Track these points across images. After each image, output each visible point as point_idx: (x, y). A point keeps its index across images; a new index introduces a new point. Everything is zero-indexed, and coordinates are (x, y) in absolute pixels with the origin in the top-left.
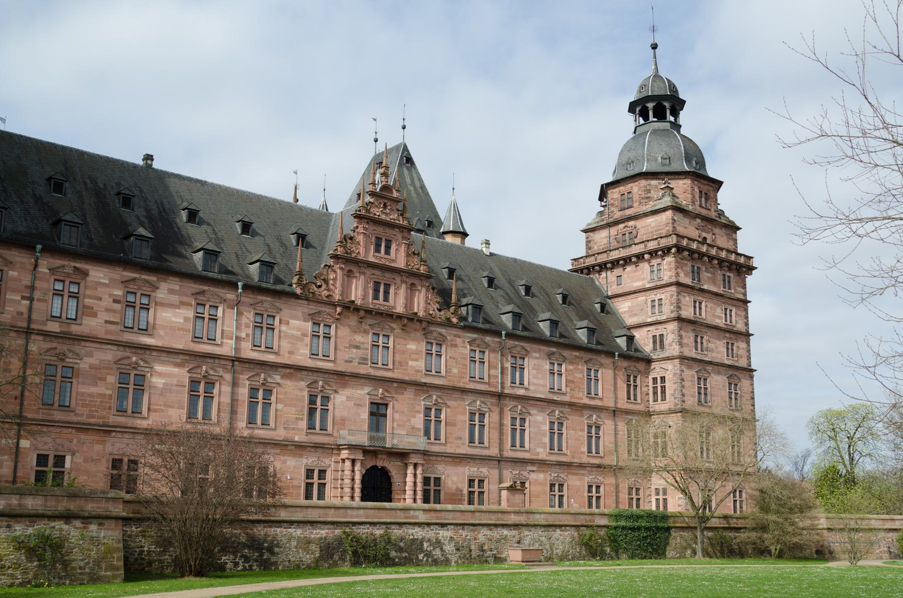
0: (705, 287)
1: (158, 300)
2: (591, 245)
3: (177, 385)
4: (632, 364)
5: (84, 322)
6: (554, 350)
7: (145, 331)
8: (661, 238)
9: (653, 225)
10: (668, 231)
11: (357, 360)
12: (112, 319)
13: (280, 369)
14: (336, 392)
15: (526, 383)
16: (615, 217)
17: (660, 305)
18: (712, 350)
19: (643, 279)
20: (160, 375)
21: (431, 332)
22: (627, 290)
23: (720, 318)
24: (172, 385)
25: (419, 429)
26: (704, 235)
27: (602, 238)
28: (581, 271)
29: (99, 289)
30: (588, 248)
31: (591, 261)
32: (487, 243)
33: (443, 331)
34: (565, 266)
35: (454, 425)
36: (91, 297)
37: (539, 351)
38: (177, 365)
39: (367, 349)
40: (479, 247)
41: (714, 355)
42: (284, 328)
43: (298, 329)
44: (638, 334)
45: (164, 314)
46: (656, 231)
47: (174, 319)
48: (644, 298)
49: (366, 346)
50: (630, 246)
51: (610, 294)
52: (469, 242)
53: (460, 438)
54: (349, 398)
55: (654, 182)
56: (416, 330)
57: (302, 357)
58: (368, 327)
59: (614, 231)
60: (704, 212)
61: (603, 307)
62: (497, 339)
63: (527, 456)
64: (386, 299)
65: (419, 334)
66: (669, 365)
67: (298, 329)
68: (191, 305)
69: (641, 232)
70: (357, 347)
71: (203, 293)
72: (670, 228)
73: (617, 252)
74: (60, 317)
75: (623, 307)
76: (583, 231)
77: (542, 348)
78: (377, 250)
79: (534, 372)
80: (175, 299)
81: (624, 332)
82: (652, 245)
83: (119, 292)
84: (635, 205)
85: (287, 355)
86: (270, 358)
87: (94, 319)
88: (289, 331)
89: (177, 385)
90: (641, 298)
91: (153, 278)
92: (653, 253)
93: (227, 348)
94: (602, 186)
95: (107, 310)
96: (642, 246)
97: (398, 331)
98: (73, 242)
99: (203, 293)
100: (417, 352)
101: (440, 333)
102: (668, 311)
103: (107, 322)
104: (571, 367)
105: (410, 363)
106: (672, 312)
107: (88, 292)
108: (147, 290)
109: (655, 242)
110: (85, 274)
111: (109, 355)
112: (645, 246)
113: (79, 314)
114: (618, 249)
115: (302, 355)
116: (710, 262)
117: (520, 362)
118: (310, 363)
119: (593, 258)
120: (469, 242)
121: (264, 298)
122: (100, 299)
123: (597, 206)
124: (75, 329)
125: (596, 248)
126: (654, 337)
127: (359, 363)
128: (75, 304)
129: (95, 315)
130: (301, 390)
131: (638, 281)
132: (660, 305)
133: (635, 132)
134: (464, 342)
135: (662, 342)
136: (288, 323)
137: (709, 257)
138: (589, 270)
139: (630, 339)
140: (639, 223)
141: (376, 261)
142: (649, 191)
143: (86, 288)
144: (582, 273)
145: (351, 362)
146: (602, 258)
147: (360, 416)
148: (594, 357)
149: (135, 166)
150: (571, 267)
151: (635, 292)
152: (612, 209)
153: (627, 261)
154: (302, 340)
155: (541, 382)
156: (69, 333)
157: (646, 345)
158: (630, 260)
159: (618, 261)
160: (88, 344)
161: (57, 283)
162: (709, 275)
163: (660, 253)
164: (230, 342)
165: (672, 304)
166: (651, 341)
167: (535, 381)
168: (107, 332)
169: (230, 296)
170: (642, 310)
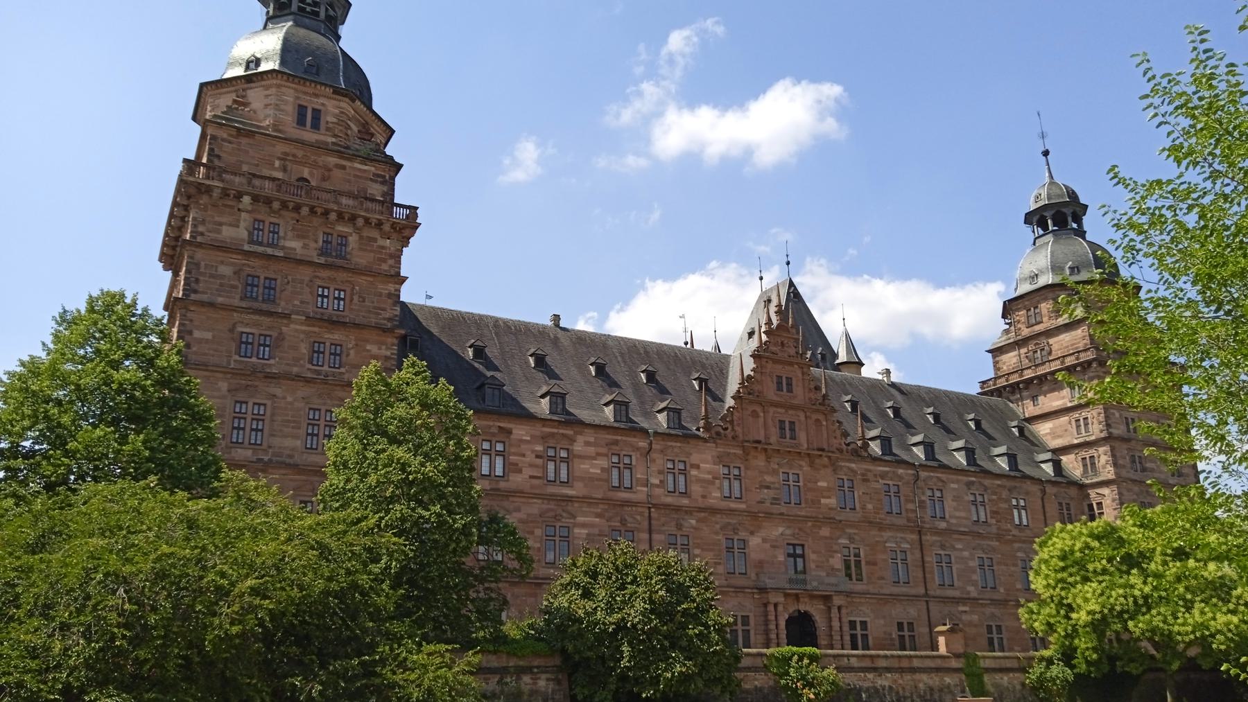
1: (575, 453)
2: (1000, 365)
3: (599, 535)
4: (1063, 490)
5: (511, 478)
6: (973, 479)
7: (566, 484)
8: (1078, 352)
9: (1067, 339)
10: (1086, 344)
11: (769, 501)
12: (535, 474)
13: (695, 514)
14: (752, 533)
15: (947, 516)
16: (1023, 334)
17: (1086, 425)
19: (1063, 398)
20: (583, 525)
21: (841, 467)
22: (1047, 411)
24: (594, 535)
25: (838, 570)
27: (1010, 360)
28: (991, 393)
29: (523, 446)
30: (997, 369)
31: (1002, 382)
32: (888, 372)
33: (853, 465)
34: (974, 389)
35: (875, 564)
36: (515, 454)
37: (957, 482)
38: (598, 515)
39: (777, 489)
40: (880, 377)
42: (694, 472)
43: (709, 473)
44: (1065, 459)
45: (582, 466)
46: (1072, 345)
47: (591, 470)
48: (1067, 418)
49: (777, 485)
50: (1043, 363)
51: (1027, 416)
52: (866, 372)
53: (882, 578)
54: (764, 540)
57: (715, 498)
58: (776, 467)
59: (1023, 351)
61: (1021, 430)
63: (957, 594)
64: (793, 438)
65: (829, 471)
66: (1105, 491)
67: (709, 473)
68: (606, 455)
69: (1055, 347)
70: (768, 487)
71: (616, 443)
72: (1087, 341)
73: (1029, 371)
74: (490, 475)
75: (1043, 429)
76: (989, 351)
78: (780, 388)
79: (955, 504)
80: (591, 450)
81: (1048, 456)
82: (1070, 361)
83: (539, 448)
84: (1045, 319)
85: (700, 499)
86: (685, 501)
87: (520, 475)
88: (702, 476)
89: (599, 535)
90: (1064, 419)
91: (570, 432)
92: (1070, 370)
93: (641, 493)
94: (1005, 302)
95: (531, 465)
96: (1058, 362)
97: (806, 468)
98: (497, 403)
99: (616, 443)
100: (828, 489)
101: (849, 468)
102: (1096, 430)
103: (531, 477)
104: (994, 497)
105: (823, 501)
106: (1101, 431)
107: (513, 450)
108: (565, 444)
109: (1073, 358)
110: (509, 432)
111: (535, 507)
112: (1063, 363)
113: (506, 471)
114: (1030, 368)
115: (716, 498)
117: (938, 494)
118: (724, 504)
119: (1003, 379)
120: (866, 372)
121: (674, 444)
122: (524, 455)
123: (1002, 325)
124: (502, 485)
125: (1005, 368)
126: (1084, 459)
127: (772, 504)
128: (502, 462)
129: (520, 471)
130: (717, 533)
131: (1058, 400)
132: (1086, 425)
133: (1034, 244)
134: (875, 476)
135: (1093, 464)
136: (698, 467)
138: (998, 392)
139: (1057, 465)
140: (1051, 341)
141: (778, 399)
143: (511, 445)
144: (992, 396)
145: (763, 503)
146: (1015, 379)
147: (776, 557)
148: (1018, 485)
149: (544, 327)
150: (980, 391)
152: (1019, 326)
153: (1042, 379)
154: (713, 483)
155: (963, 514)
156: (498, 490)
157: (1074, 468)
158: (1046, 378)
159: (1031, 379)
160: (515, 499)
161: (484, 443)
163: (1078, 369)
164: (645, 489)
165: (1100, 423)
166: (1081, 464)
168: (532, 487)
169: (643, 444)
170: (1066, 430)
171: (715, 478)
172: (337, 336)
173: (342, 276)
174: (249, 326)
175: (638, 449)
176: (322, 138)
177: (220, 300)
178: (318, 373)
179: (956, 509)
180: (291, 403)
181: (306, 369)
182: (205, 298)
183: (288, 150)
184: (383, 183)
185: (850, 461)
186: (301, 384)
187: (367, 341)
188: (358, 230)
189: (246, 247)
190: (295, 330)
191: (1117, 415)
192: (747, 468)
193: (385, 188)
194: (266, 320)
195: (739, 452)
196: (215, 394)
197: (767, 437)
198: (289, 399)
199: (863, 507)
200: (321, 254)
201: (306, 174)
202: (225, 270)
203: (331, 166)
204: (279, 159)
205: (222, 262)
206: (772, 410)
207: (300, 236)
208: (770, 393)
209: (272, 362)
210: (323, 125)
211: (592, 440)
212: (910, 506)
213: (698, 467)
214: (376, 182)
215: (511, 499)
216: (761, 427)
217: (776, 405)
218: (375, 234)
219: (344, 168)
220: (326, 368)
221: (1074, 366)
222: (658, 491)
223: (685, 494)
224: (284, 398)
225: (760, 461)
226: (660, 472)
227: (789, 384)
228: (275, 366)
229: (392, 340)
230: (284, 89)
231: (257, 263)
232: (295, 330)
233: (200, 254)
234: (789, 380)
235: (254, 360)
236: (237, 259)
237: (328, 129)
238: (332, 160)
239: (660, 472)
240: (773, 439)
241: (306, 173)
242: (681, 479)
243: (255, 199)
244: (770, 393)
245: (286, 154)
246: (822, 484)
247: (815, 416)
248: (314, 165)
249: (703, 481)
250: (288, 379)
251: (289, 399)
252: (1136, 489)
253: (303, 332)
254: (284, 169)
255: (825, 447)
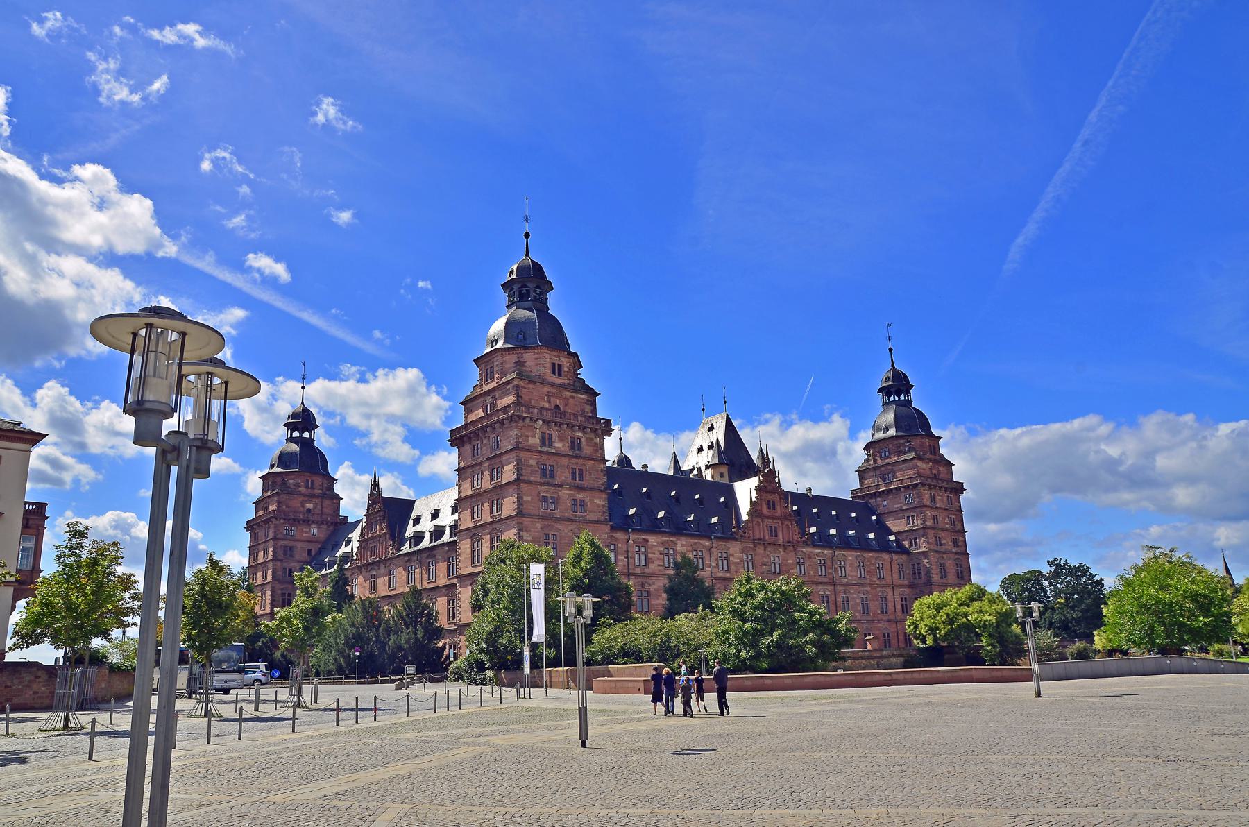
0: (938, 506)
6: (859, 554)
18: (945, 545)
19: (901, 503)
23: (947, 523)
26: (934, 472)
41: (947, 547)
55: (902, 441)
56: (791, 551)
60: (933, 457)
62: (830, 552)
64: (776, 536)
70: (765, 565)
77: (853, 553)
91: (674, 539)
100: (793, 564)
103: (659, 565)
104: (869, 563)
116: (940, 490)
122: (654, 554)
124: (646, 570)
129: (653, 562)
131: (898, 504)
134: (814, 555)
136: (732, 555)
137: (939, 487)
142: (899, 447)
151: (895, 511)
160: (652, 578)
162: (940, 497)
167: (852, 574)
168: (660, 571)
171: (741, 561)
172: (581, 496)
173: (581, 461)
174: (547, 492)
175: (704, 547)
176: (563, 381)
177: (532, 479)
178: (575, 516)
179: (851, 571)
180: (567, 534)
181: (569, 514)
182: (526, 478)
183: (549, 390)
184: (591, 405)
185: (803, 547)
186: (570, 523)
187: (594, 497)
188: (585, 433)
189: (540, 449)
190: (564, 493)
191: (929, 514)
192: (755, 555)
193: (592, 408)
194: (552, 489)
195: (752, 546)
196: (536, 530)
197: (764, 537)
198: (566, 531)
199: (809, 573)
200: (572, 447)
201: (558, 404)
202: (533, 462)
203: (568, 397)
204: (546, 395)
205: (531, 458)
206: (766, 520)
207: (562, 439)
208: (765, 510)
209: (556, 511)
210: (563, 375)
211: (684, 543)
212: (830, 571)
213: (732, 555)
214: (588, 404)
215: (650, 578)
216: (761, 532)
217: (768, 517)
218: (592, 436)
219: (573, 397)
220: (578, 513)
221: (908, 486)
222: (715, 570)
223: (728, 571)
224: (564, 531)
225: (760, 550)
226: (716, 559)
227: (774, 505)
228: (558, 513)
229: (604, 496)
230: (545, 354)
231: (545, 457)
232: (564, 493)
233: (522, 454)
234: (773, 502)
235: (549, 510)
236: (536, 455)
237: (566, 376)
238: (569, 394)
239: (716, 559)
240: (767, 538)
241: (558, 402)
242: (725, 562)
243: (544, 421)
244: (765, 510)
245: (548, 392)
246: (790, 561)
247: (787, 523)
248: (561, 397)
249: (736, 563)
250: (563, 520)
251: (566, 531)
252: (937, 556)
253: (569, 494)
254: (549, 402)
255: (791, 540)
